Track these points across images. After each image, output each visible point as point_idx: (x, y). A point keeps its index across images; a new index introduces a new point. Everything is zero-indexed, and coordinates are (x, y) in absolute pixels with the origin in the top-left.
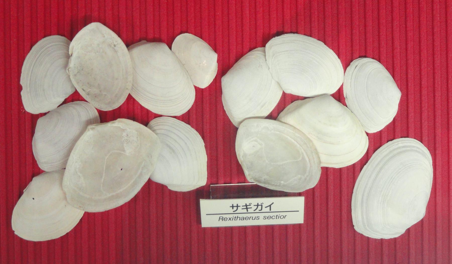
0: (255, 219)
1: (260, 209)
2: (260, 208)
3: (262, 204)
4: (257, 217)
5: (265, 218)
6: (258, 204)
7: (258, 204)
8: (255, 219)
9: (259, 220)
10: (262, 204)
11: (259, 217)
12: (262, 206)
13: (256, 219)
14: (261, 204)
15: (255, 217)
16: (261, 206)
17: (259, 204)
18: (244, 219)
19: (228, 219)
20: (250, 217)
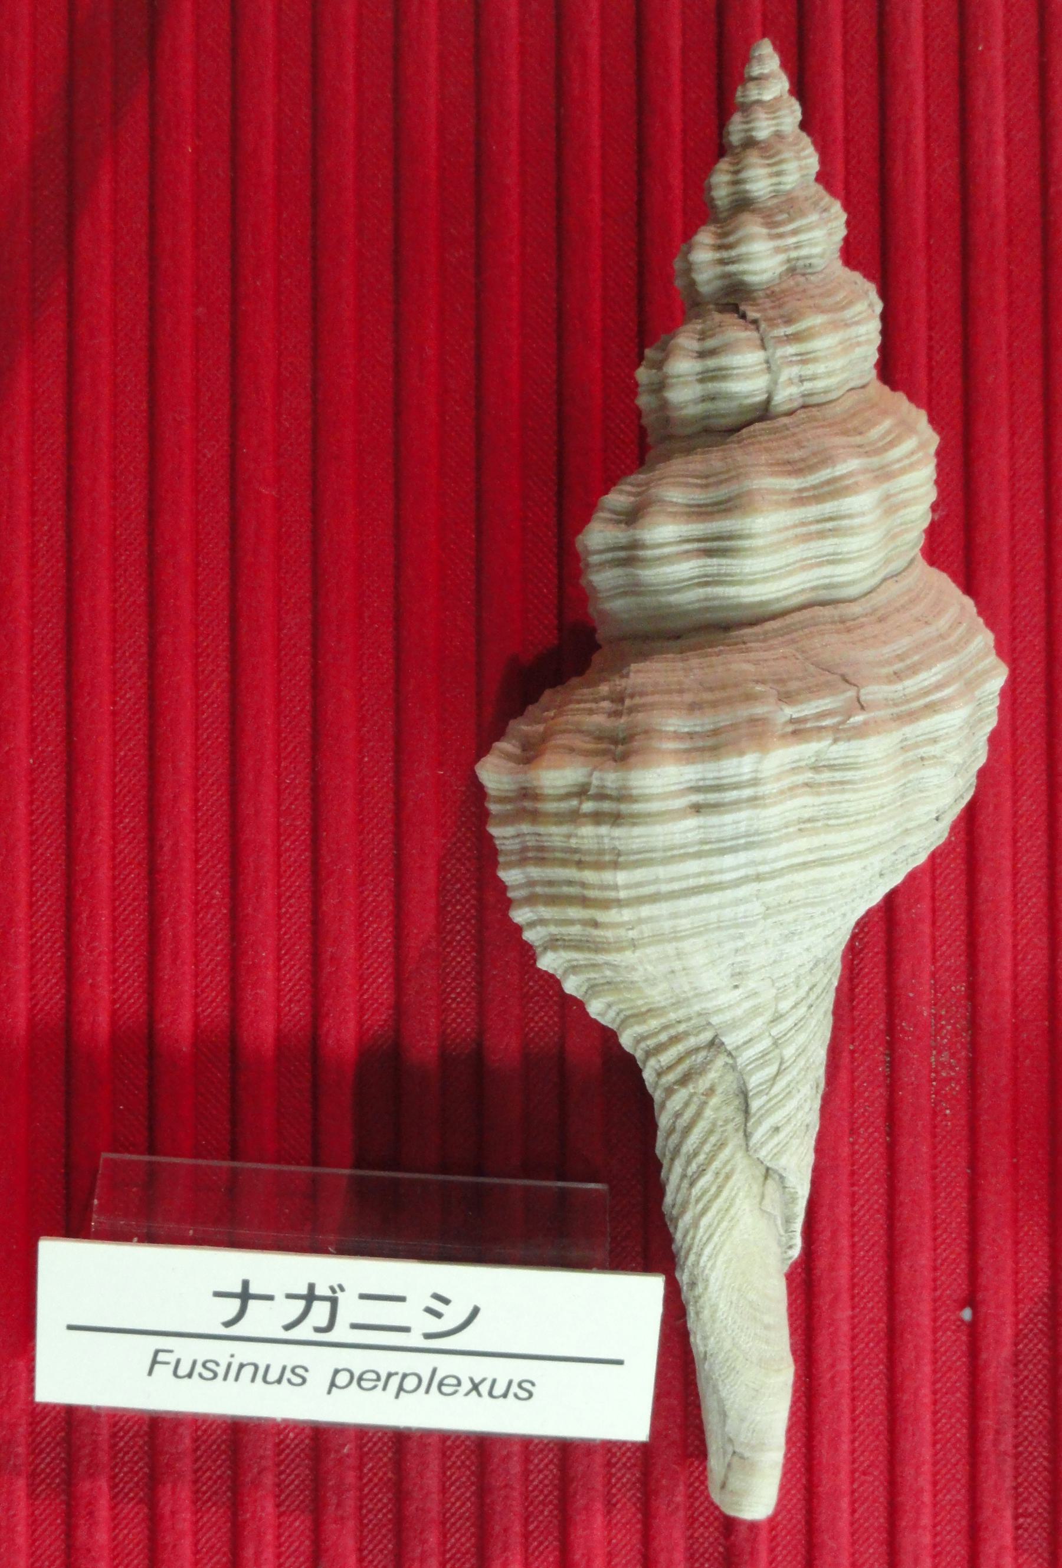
0: (190, 1375)
1: (324, 1323)
4: (204, 1365)
5: (210, 1375)
6: (311, 1287)
7: (311, 1287)
8: (190, 1375)
9: (303, 1387)
10: (339, 1294)
11: (533, 1384)
12: (334, 1302)
13: (511, 1395)
14: (328, 1293)
15: (195, 1363)
16: (327, 1305)
17: (318, 1292)
18: (209, 1370)
19: (467, 1385)
20: (390, 1375)
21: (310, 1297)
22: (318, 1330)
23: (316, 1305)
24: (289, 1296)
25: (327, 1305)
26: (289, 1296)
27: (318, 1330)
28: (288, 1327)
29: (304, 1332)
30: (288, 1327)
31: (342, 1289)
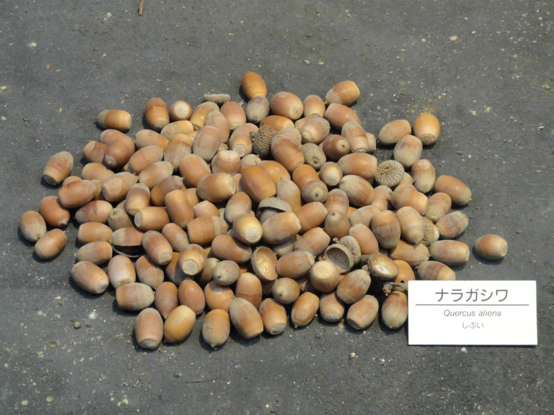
1: (475, 299)
2: (474, 295)
3: (476, 290)
6: (471, 290)
7: (471, 290)
10: (477, 291)
12: (476, 293)
14: (475, 291)
16: (475, 294)
17: (473, 291)
21: (471, 293)
22: (474, 301)
23: (473, 294)
24: (467, 293)
25: (475, 294)
26: (467, 293)
27: (474, 301)
28: (467, 301)
29: (470, 302)
30: (467, 301)
31: (478, 290)
